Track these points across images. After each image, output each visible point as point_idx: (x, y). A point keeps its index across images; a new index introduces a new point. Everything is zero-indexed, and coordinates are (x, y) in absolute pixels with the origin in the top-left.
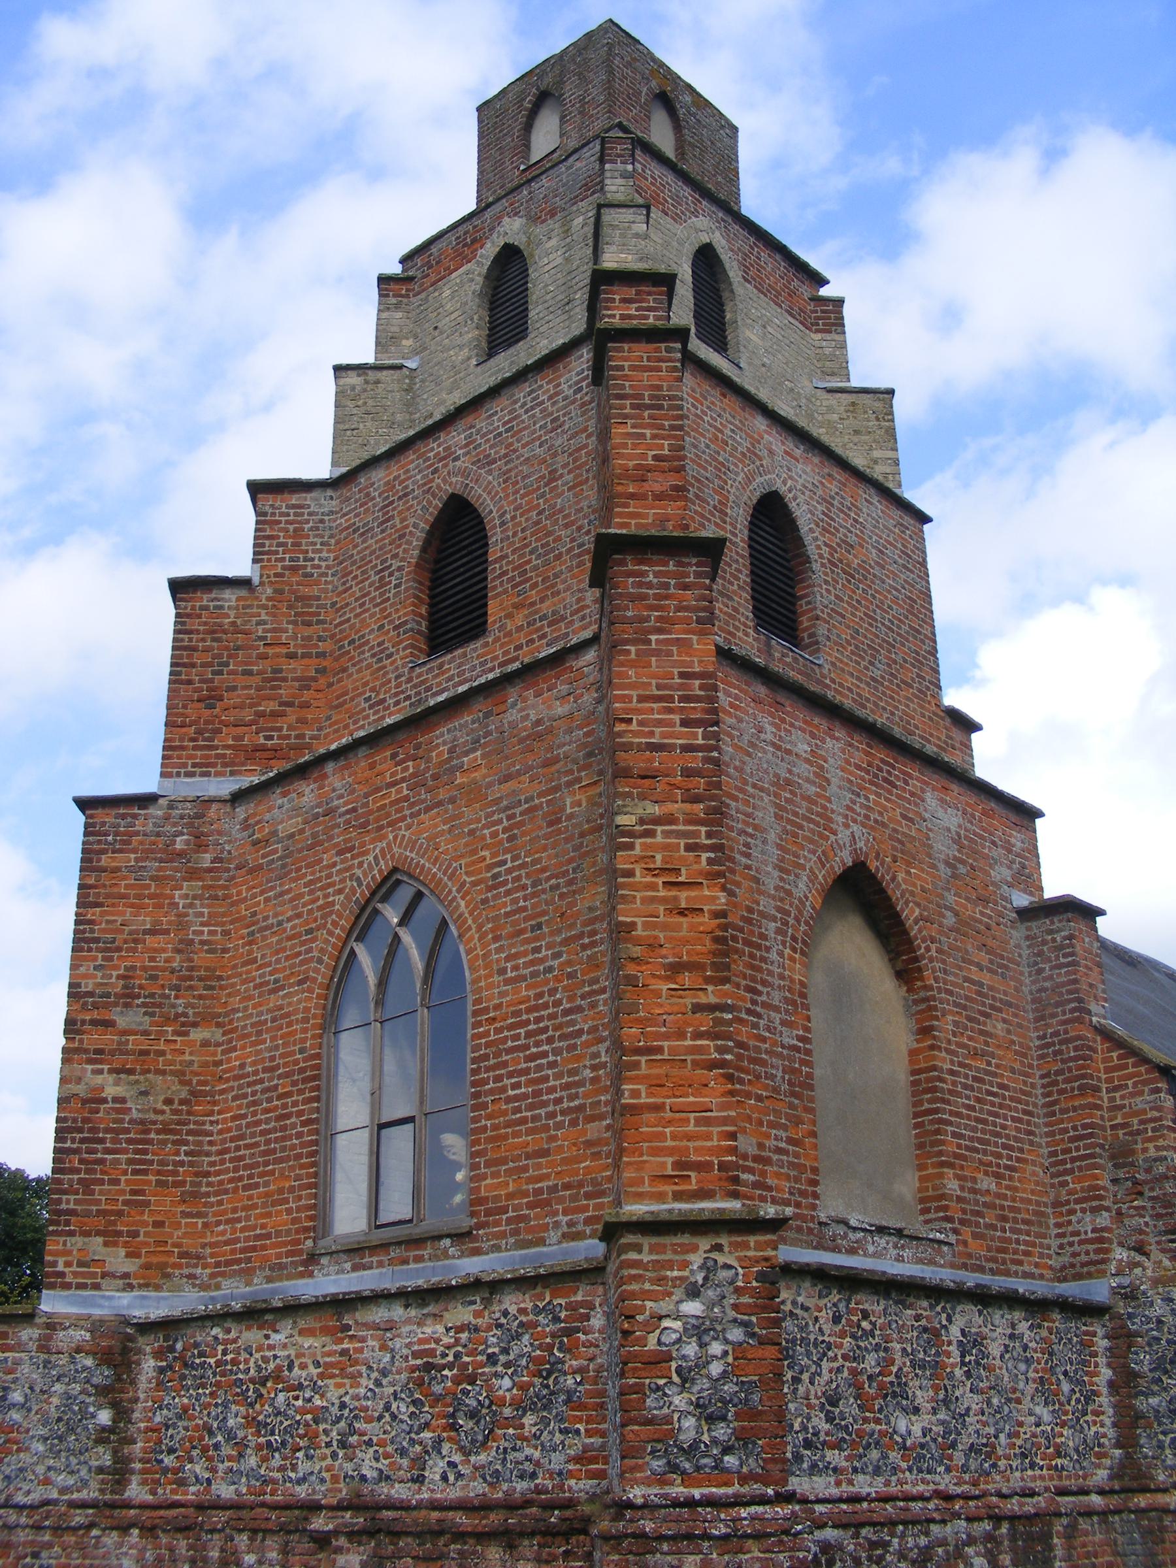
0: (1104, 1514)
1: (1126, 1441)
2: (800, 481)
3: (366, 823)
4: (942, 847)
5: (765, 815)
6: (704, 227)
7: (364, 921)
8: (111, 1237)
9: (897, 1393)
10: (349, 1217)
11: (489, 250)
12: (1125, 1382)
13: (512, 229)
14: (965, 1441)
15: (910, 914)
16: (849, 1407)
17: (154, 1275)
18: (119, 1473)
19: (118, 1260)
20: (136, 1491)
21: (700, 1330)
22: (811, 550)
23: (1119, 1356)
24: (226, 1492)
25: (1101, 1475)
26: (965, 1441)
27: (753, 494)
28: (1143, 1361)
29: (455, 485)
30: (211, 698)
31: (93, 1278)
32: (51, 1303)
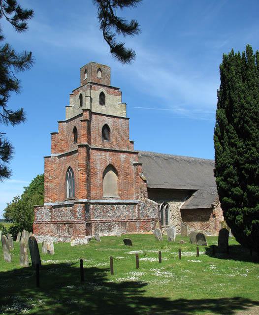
0: (134, 221)
1: (138, 215)
2: (109, 122)
3: (68, 161)
4: (122, 159)
5: (98, 162)
6: (102, 89)
7: (68, 171)
8: (50, 198)
9: (108, 212)
10: (68, 197)
11: (79, 94)
12: (139, 210)
13: (81, 92)
14: (116, 215)
15: (117, 168)
16: (102, 213)
17: (54, 201)
18: (52, 219)
19: (50, 200)
20: (53, 220)
21: (79, 210)
22: (111, 129)
23: (138, 207)
24: (59, 220)
25: (135, 218)
26: (116, 215)
27: (104, 124)
28: (140, 208)
29: (75, 125)
30: (55, 145)
31: (48, 202)
32: (45, 204)
